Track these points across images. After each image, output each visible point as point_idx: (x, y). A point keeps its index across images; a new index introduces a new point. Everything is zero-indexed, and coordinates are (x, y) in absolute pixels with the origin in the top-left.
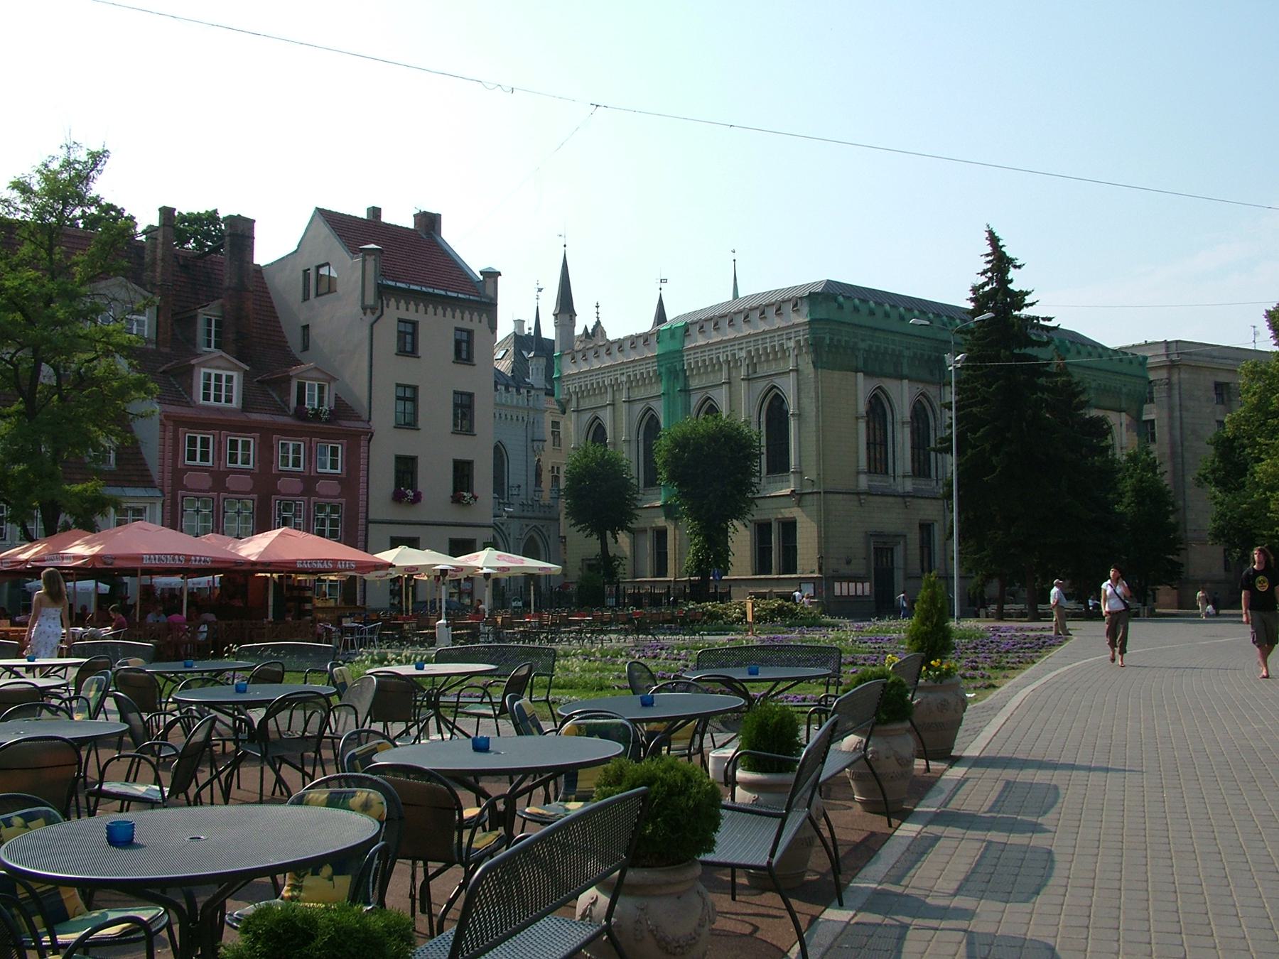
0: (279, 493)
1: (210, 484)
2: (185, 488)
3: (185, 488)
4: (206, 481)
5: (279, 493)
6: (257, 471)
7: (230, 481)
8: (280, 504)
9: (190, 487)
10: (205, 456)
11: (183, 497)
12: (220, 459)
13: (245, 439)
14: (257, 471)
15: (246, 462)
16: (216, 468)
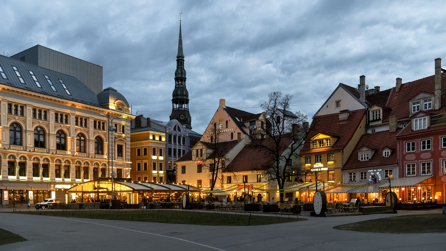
0: (442, 157)
1: (415, 158)
2: (406, 160)
3: (406, 160)
4: (413, 157)
5: (442, 157)
6: (433, 150)
7: (422, 156)
8: (443, 161)
9: (408, 160)
10: (413, 149)
11: (406, 164)
12: (418, 149)
13: (427, 140)
14: (433, 150)
15: (429, 147)
16: (417, 152)
